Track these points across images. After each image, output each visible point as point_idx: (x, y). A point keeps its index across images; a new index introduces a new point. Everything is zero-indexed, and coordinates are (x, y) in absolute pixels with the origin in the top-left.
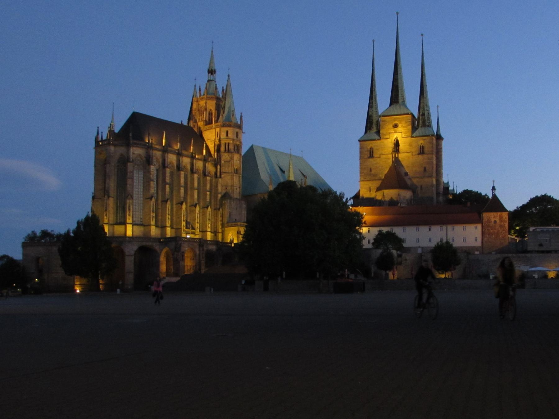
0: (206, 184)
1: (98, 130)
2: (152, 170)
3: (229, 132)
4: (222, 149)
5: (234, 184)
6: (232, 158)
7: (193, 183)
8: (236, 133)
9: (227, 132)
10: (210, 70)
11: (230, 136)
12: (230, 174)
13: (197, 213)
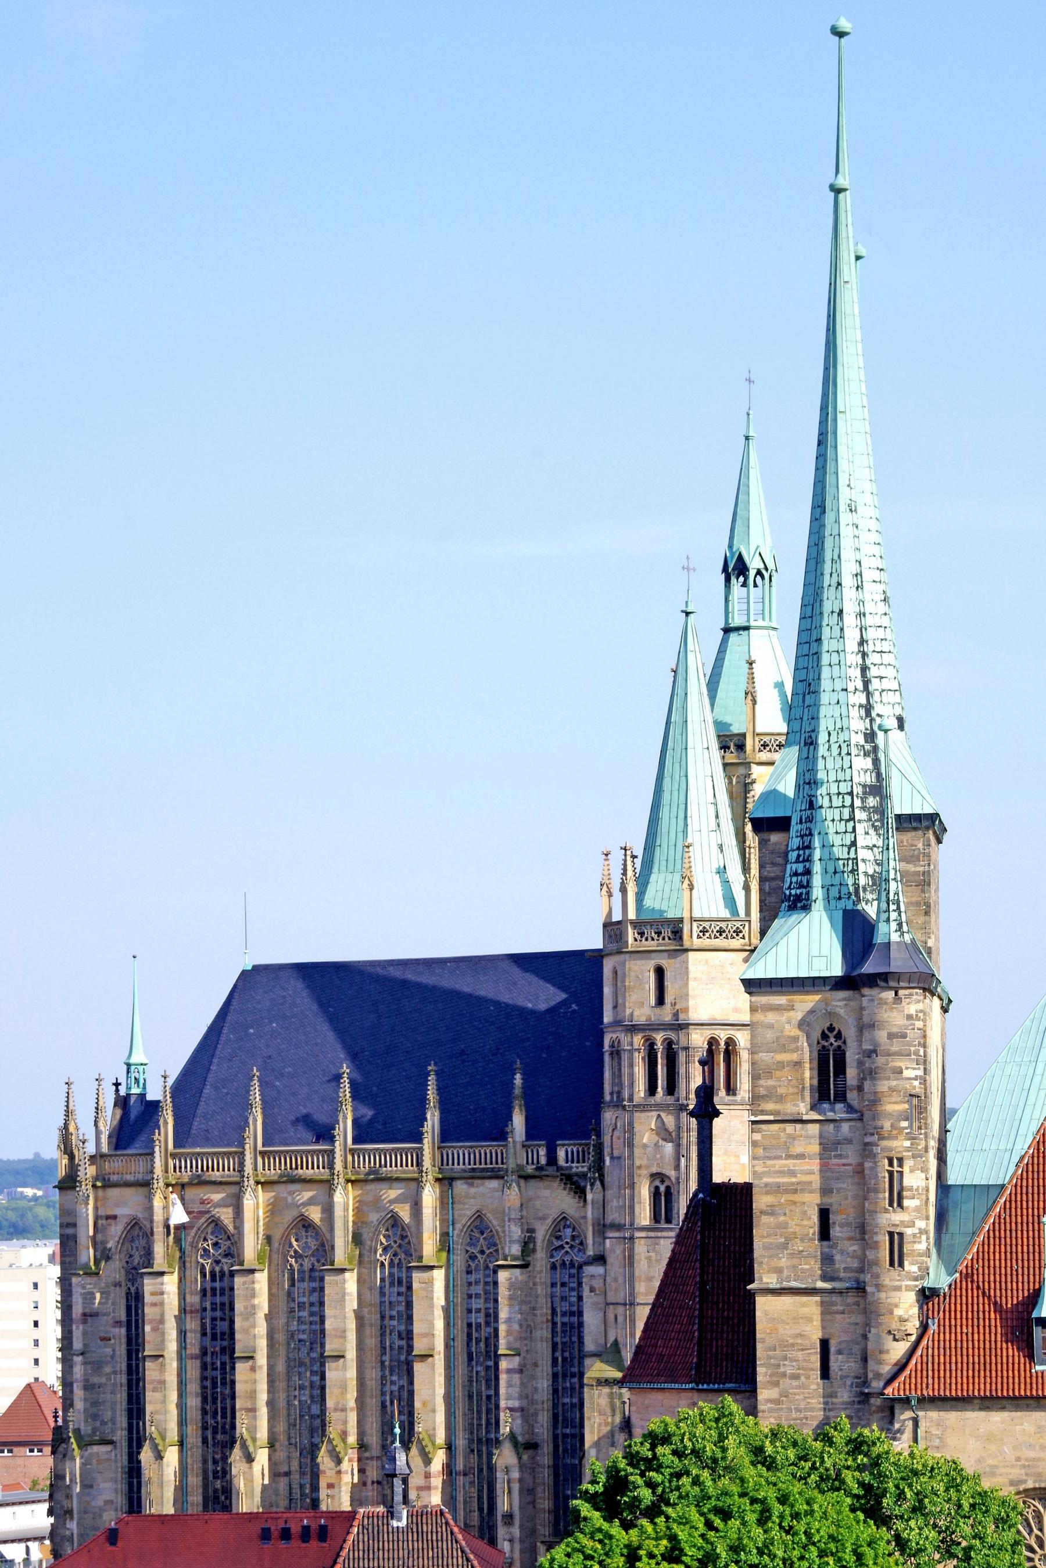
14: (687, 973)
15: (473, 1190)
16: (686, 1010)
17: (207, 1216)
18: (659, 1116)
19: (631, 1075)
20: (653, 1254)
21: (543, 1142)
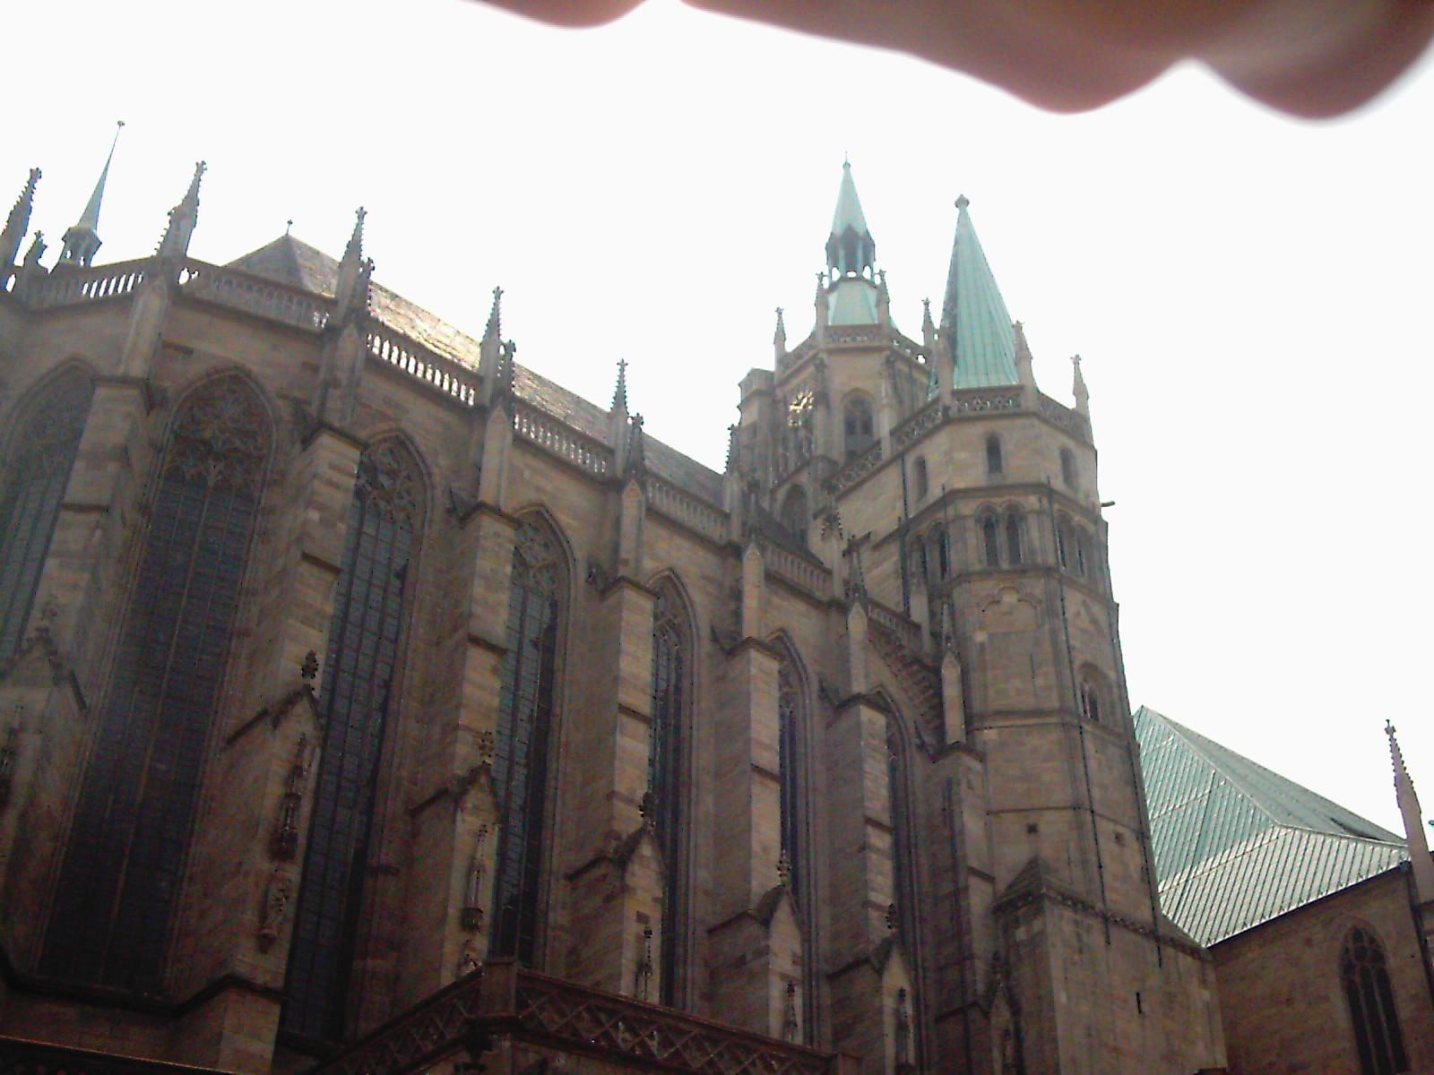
0: (857, 764)
3: (1007, 447)
4: (968, 549)
5: (1096, 793)
7: (735, 729)
8: (1056, 454)
10: (839, 232)
12: (1054, 720)
13: (784, 976)
15: (776, 600)
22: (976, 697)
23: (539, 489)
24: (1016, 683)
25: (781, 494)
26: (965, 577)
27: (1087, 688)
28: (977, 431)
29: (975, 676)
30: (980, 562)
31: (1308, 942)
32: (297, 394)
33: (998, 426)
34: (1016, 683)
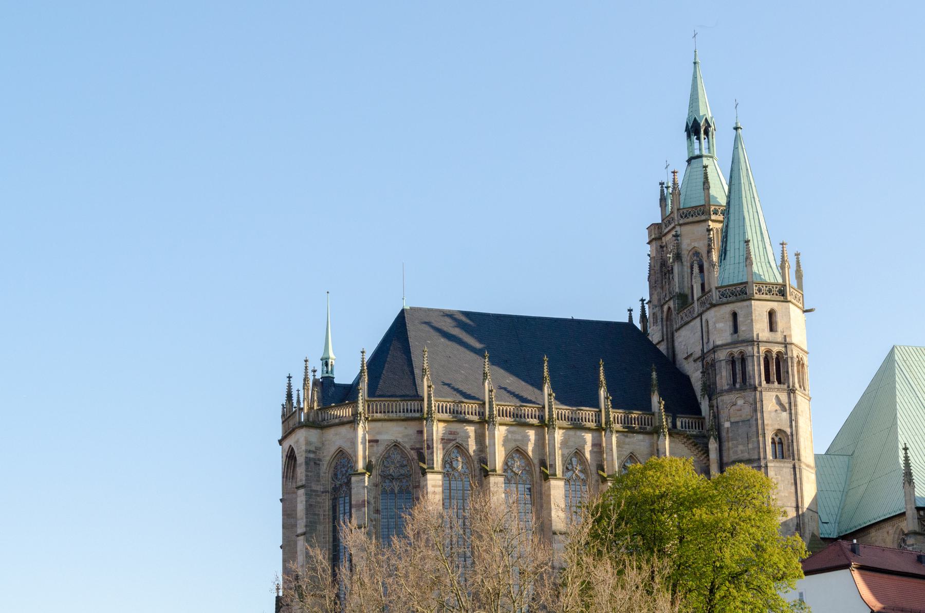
1: (289, 386)
2: (433, 486)
3: (740, 319)
4: (723, 377)
6: (756, 407)
9: (735, 315)
11: (743, 329)
14: (789, 315)
15: (627, 440)
16: (790, 336)
17: (454, 442)
18: (777, 396)
19: (760, 370)
20: (779, 477)
21: (671, 414)
22: (725, 454)
23: (515, 440)
24: (741, 447)
25: (666, 308)
26: (722, 392)
27: (777, 439)
28: (726, 310)
29: (726, 445)
30: (727, 385)
31: (888, 533)
32: (418, 446)
33: (737, 307)
34: (741, 447)
